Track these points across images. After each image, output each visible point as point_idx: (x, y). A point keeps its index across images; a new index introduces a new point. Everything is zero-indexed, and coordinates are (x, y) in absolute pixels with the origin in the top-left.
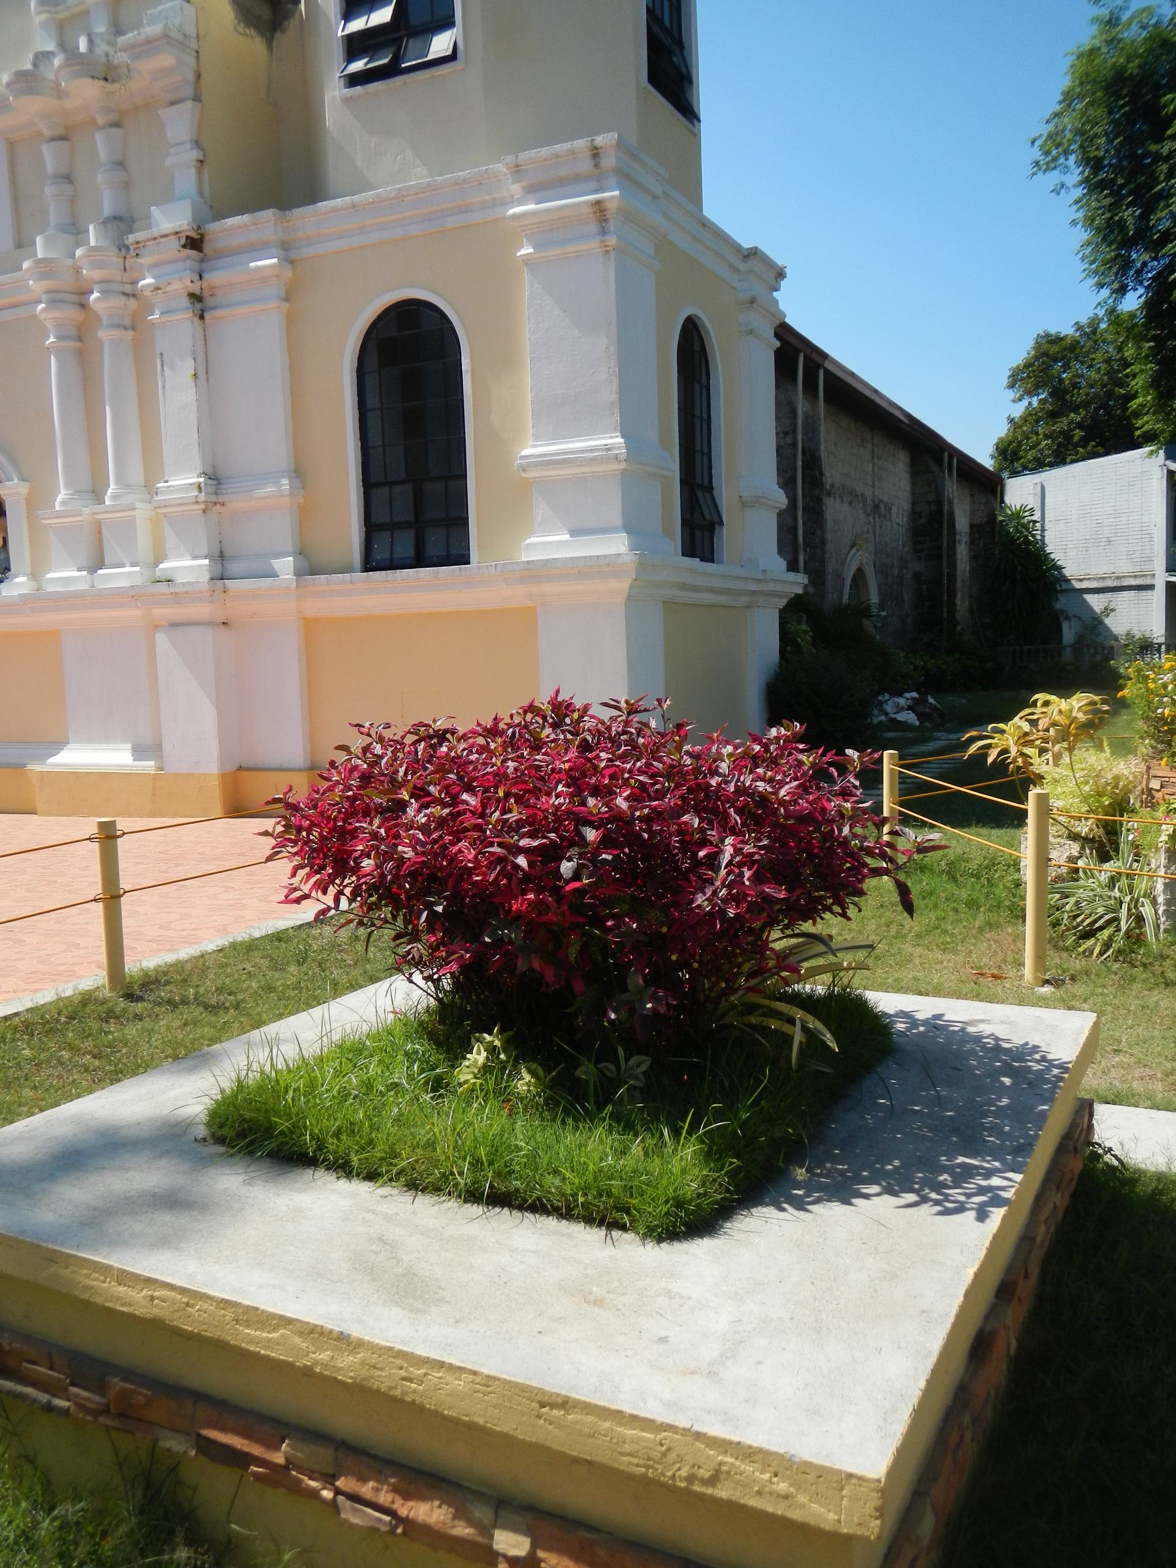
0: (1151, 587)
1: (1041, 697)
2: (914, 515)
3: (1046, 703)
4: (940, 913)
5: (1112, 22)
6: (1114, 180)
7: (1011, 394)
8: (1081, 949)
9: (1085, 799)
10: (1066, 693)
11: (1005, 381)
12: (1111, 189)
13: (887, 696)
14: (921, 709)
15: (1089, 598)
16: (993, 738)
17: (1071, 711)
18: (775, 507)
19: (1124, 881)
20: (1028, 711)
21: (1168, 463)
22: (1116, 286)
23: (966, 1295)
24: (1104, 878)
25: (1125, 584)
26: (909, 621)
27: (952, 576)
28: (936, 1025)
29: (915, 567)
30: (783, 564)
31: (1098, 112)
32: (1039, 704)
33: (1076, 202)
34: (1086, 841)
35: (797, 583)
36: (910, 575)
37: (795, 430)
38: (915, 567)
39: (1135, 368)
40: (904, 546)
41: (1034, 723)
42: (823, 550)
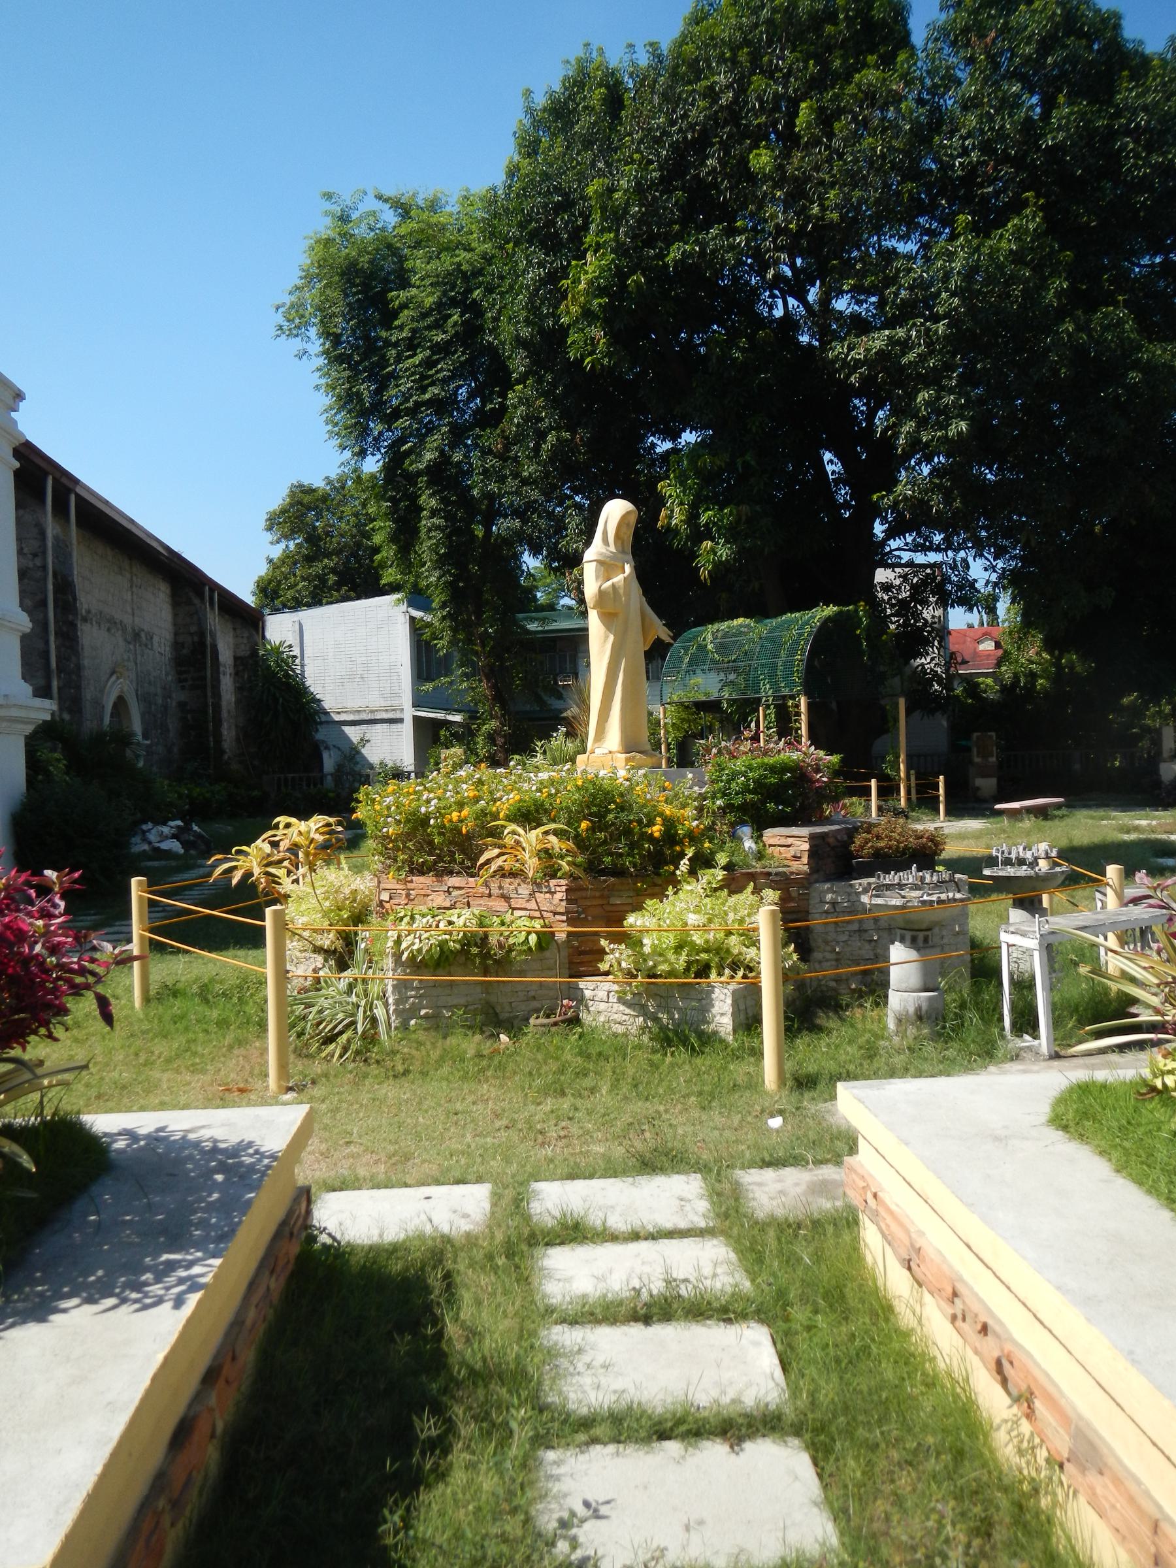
0: (400, 721)
1: (282, 820)
2: (177, 645)
3: (288, 826)
4: (191, 1035)
5: (344, 218)
6: (350, 356)
7: (269, 537)
8: (323, 1055)
9: (325, 914)
10: (304, 816)
11: (262, 523)
12: (349, 364)
13: (150, 825)
14: (186, 837)
15: (346, 729)
16: (238, 860)
17: (309, 832)
18: (19, 631)
19: (360, 988)
20: (270, 833)
21: (410, 609)
22: (357, 449)
23: (155, 1379)
24: (343, 985)
25: (378, 717)
26: (175, 750)
27: (217, 707)
28: (157, 1138)
29: (179, 696)
30: (27, 689)
31: (335, 294)
32: (281, 826)
33: (318, 370)
34: (327, 953)
35: (44, 710)
36: (174, 704)
37: (44, 552)
38: (179, 696)
39: (377, 524)
40: (167, 674)
41: (275, 845)
42: (79, 676)
